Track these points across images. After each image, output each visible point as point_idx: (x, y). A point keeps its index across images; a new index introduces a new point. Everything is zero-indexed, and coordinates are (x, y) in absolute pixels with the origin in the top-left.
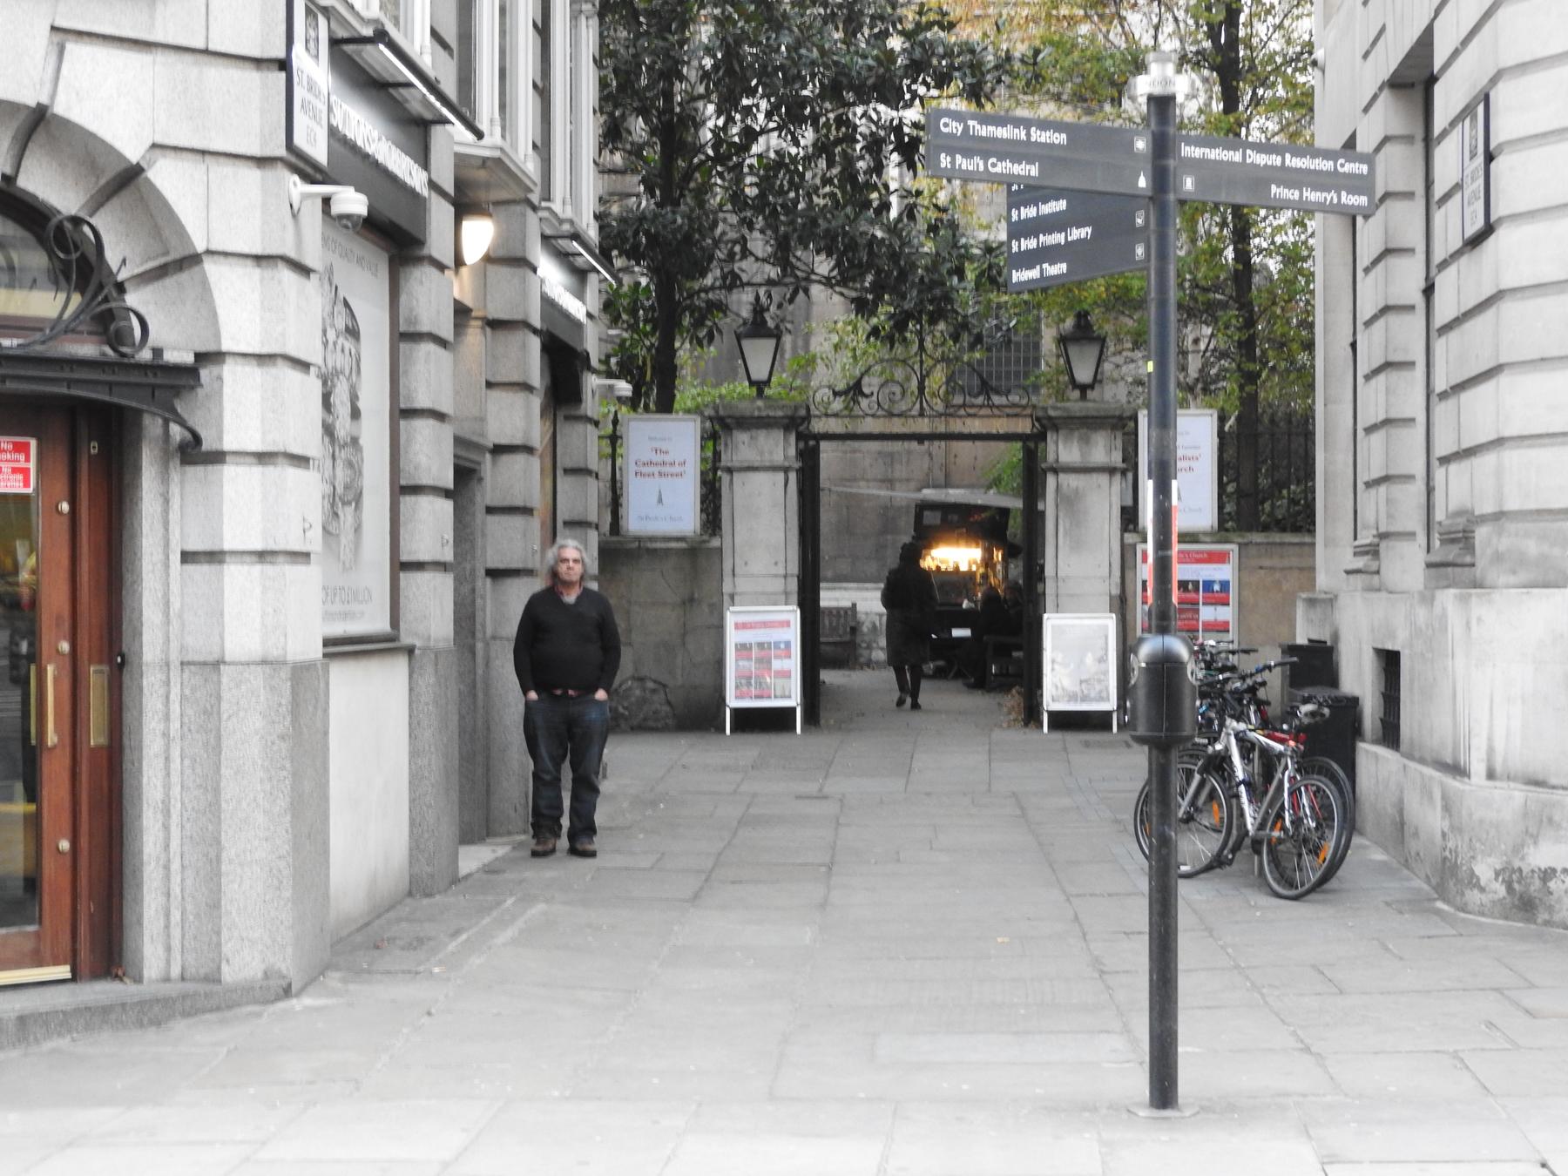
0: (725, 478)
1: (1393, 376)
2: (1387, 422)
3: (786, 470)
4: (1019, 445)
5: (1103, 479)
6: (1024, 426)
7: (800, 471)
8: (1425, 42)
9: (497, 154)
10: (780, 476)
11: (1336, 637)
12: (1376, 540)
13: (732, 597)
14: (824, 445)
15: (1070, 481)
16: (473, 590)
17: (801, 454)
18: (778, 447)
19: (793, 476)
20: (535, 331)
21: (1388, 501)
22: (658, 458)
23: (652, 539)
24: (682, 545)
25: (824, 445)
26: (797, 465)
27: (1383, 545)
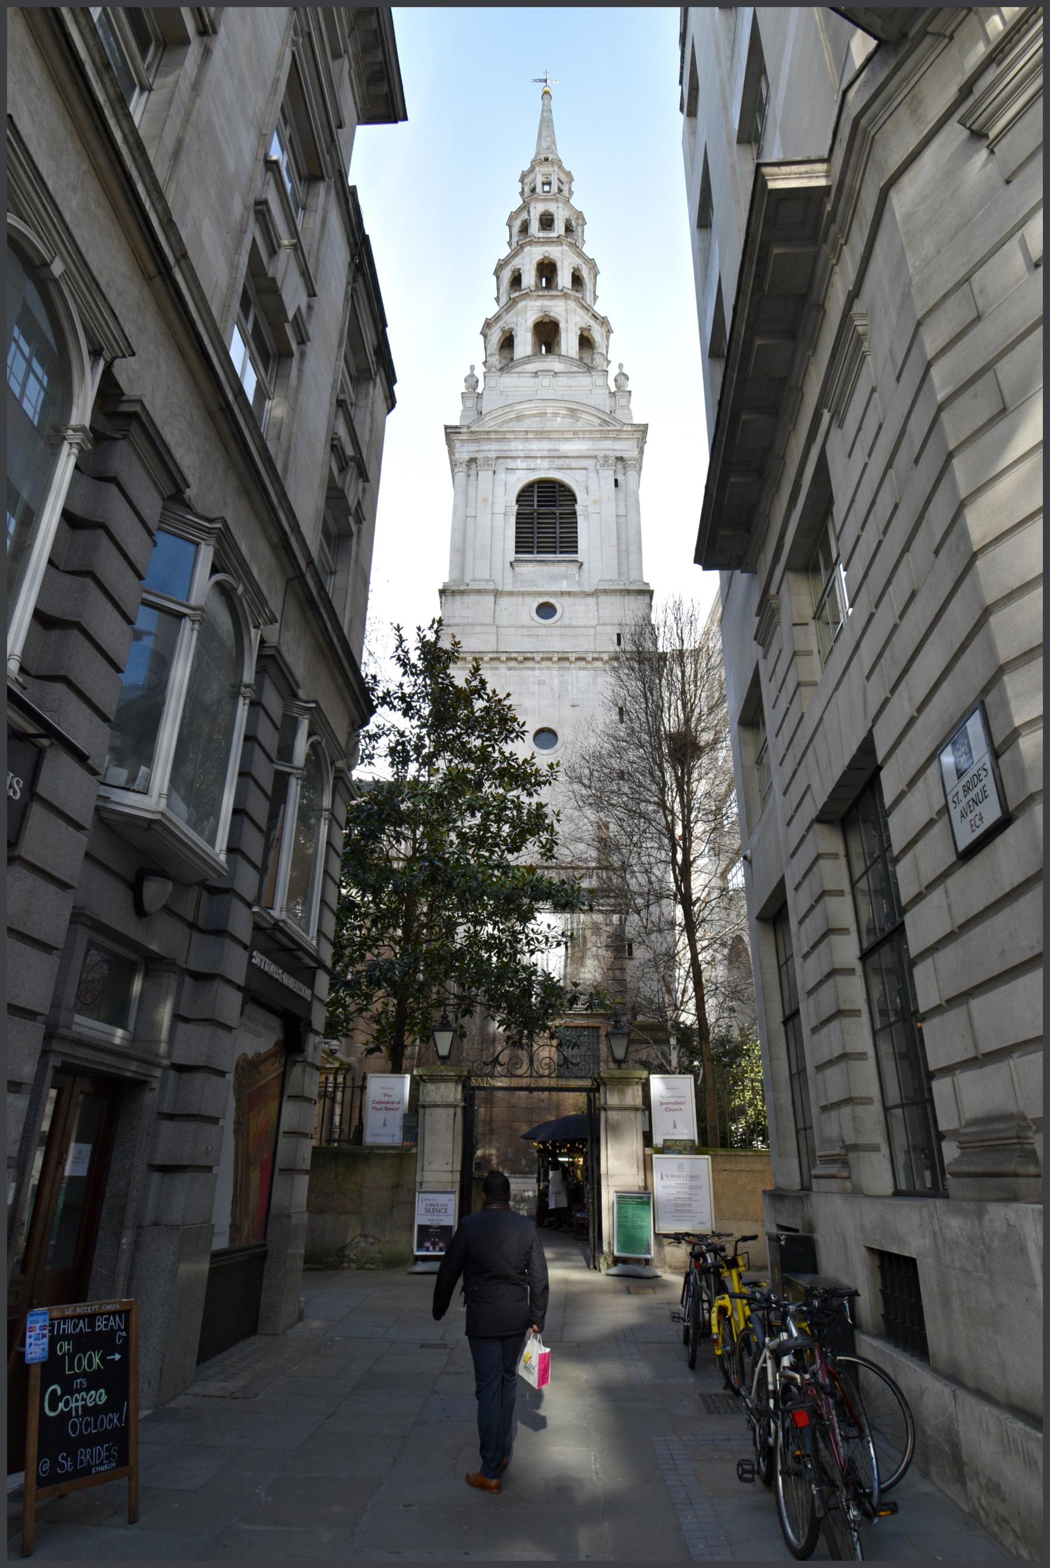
0: (421, 1111)
1: (846, 1021)
2: (844, 1057)
3: (455, 1107)
4: (584, 1094)
5: (631, 1114)
6: (587, 1083)
7: (464, 1109)
8: (868, 746)
9: (158, 817)
10: (452, 1111)
11: (810, 1226)
12: (844, 1152)
13: (421, 1183)
14: (477, 1092)
15: (613, 1115)
16: (129, 1184)
17: (465, 1099)
18: (452, 1093)
19: (459, 1111)
20: (239, 988)
21: (854, 1118)
22: (386, 1099)
23: (379, 1147)
24: (394, 1152)
25: (477, 1092)
26: (463, 1104)
27: (852, 1156)
